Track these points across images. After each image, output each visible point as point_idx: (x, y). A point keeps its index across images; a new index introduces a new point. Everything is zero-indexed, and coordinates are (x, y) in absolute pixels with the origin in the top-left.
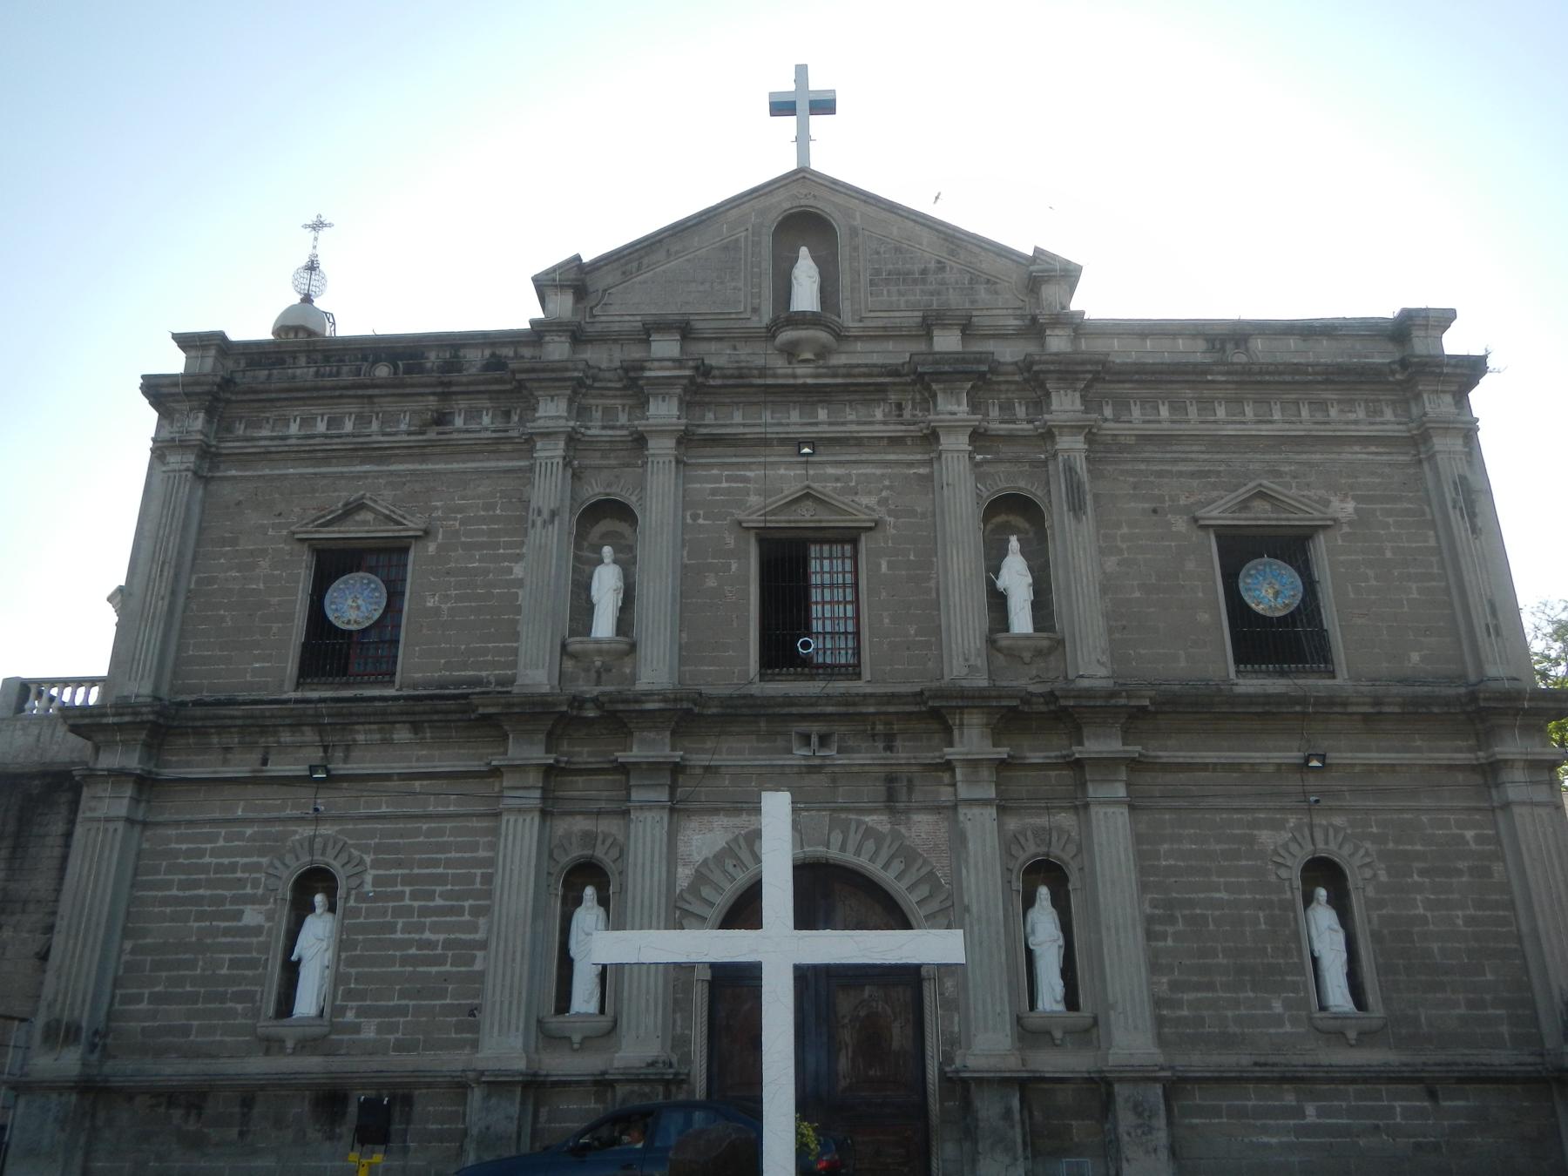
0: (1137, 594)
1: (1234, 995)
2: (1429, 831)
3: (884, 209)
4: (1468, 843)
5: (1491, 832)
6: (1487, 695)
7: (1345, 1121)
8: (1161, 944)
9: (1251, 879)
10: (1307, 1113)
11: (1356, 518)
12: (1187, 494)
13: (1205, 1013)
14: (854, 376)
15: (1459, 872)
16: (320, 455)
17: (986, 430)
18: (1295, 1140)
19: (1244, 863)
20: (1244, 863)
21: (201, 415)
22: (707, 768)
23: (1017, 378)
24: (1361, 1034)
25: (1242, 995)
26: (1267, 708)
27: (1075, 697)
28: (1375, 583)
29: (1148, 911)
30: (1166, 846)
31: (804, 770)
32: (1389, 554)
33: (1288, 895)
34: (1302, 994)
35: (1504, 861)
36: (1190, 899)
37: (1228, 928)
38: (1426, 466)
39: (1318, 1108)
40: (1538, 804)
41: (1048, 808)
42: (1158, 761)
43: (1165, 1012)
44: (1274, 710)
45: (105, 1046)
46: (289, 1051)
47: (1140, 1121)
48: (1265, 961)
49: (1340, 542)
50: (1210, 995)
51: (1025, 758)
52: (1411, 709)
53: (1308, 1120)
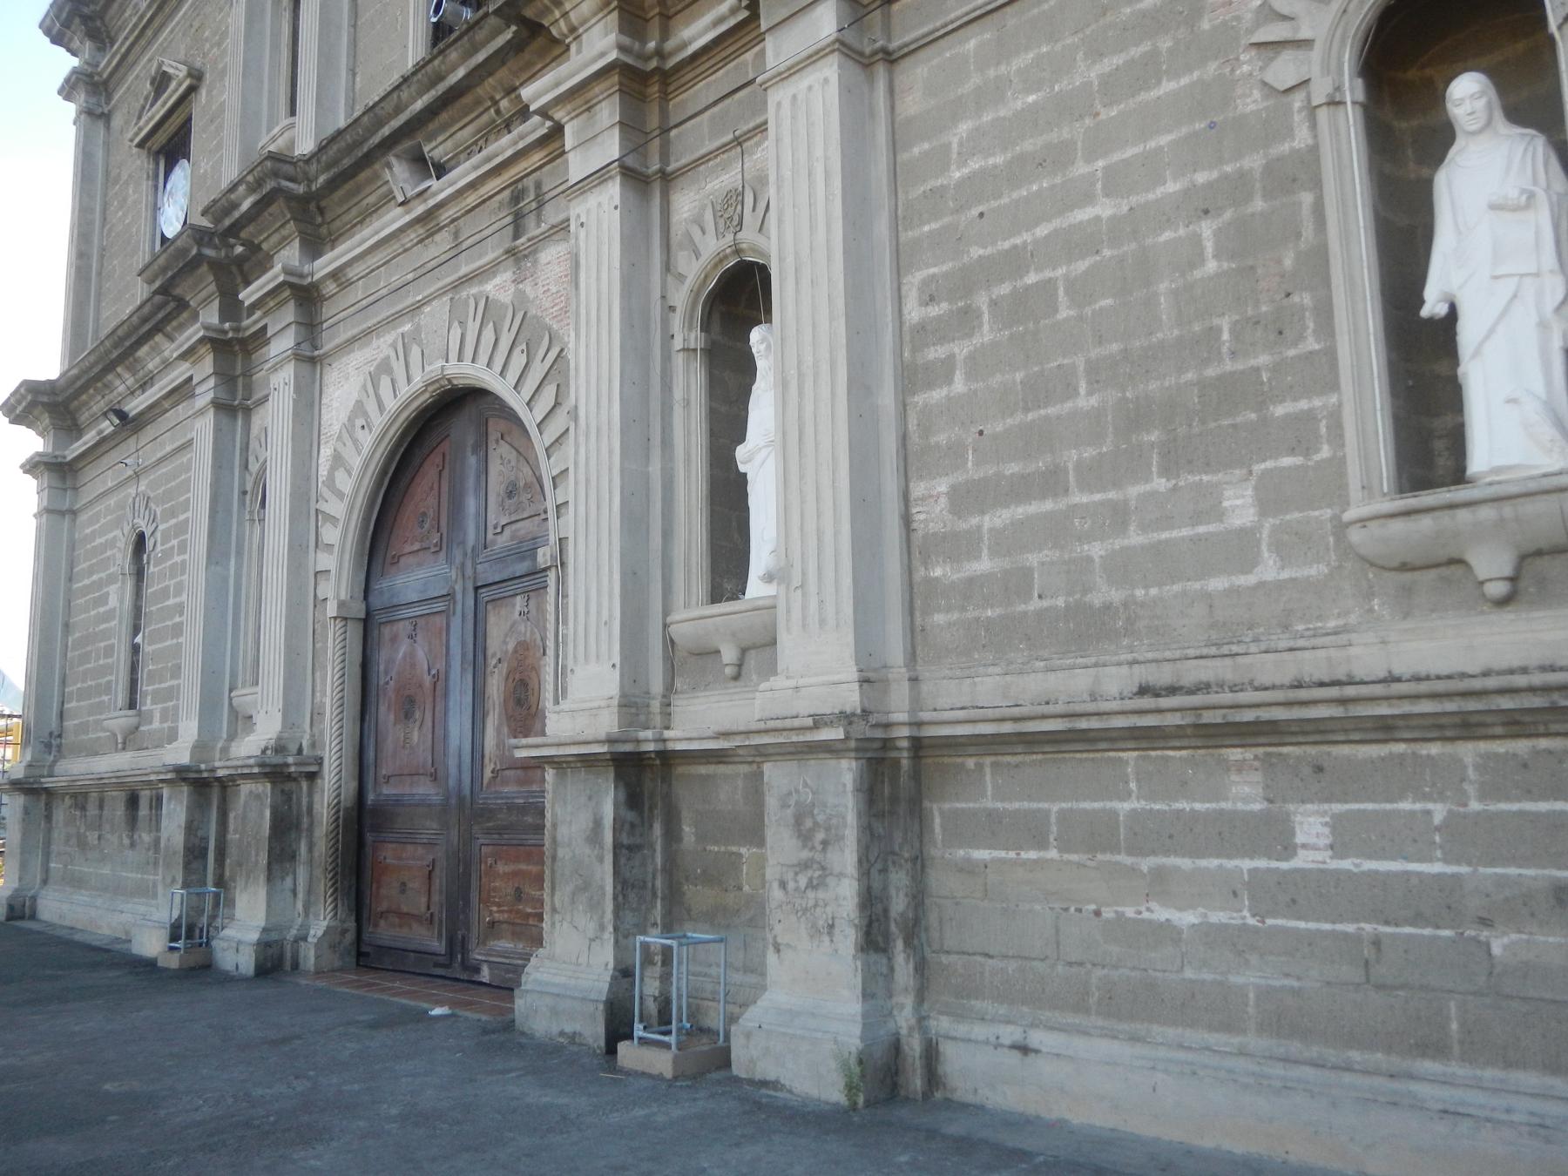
1: (1112, 495)
7: (1437, 868)
8: (937, 395)
9: (1184, 130)
10: (1300, 838)
13: (1033, 559)
16: (149, 33)
18: (1251, 921)
19: (1168, 86)
20: (1168, 86)
21: (88, 44)
22: (335, 275)
24: (1527, 557)
25: (1134, 491)
29: (914, 313)
30: (964, 128)
31: (420, 231)
33: (1302, 138)
34: (1325, 452)
36: (1015, 247)
37: (1108, 302)
39: (1338, 824)
41: (738, 142)
43: (938, 572)
45: (59, 746)
46: (120, 746)
47: (805, 854)
48: (1211, 372)
50: (1048, 505)
51: (684, 45)
53: (1304, 860)
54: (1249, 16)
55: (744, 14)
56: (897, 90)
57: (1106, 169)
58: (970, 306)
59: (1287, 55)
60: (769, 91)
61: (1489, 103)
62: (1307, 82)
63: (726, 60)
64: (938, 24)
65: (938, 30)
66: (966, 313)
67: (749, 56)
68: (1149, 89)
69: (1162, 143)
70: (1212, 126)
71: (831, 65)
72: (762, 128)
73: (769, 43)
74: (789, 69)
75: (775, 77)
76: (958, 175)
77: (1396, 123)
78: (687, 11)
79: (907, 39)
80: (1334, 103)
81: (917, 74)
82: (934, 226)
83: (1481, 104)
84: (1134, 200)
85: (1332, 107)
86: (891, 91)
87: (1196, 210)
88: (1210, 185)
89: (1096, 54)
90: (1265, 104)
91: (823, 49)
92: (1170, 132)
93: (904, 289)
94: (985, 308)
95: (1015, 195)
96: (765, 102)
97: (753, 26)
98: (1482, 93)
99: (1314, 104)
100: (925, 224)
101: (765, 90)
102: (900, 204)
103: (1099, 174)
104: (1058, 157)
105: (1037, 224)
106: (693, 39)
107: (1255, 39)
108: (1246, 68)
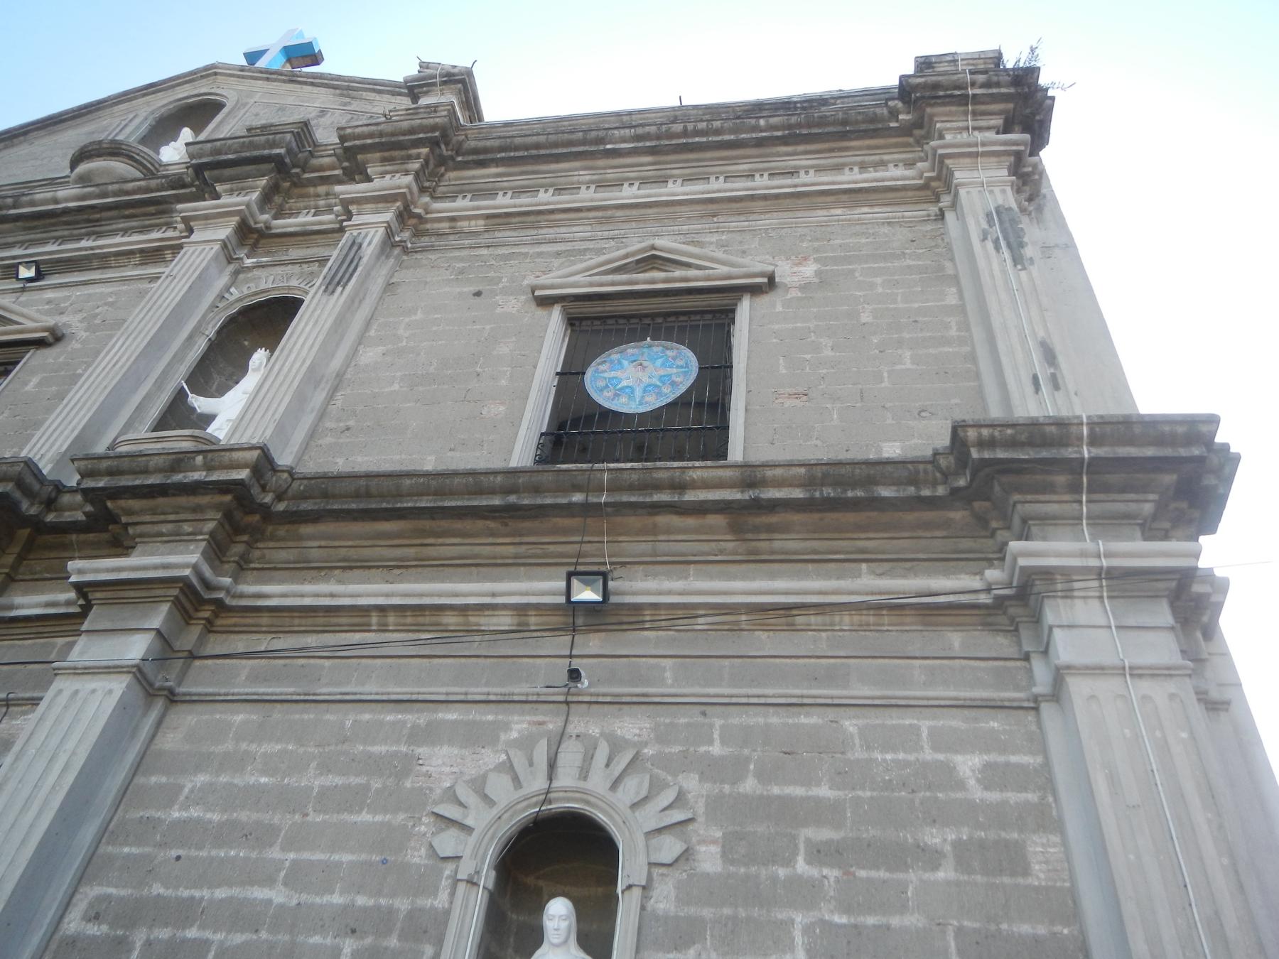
0: (396, 387)
2: (858, 754)
3: (284, 81)
4: (961, 785)
5: (1026, 759)
6: (985, 432)
9: (364, 857)
11: (816, 280)
12: (537, 274)
14: (127, 193)
15: (932, 858)
17: (268, 228)
19: (365, 817)
20: (365, 817)
23: (336, 172)
26: (512, 499)
27: (111, 473)
28: (831, 353)
29: (74, 924)
30: (202, 779)
32: (865, 318)
33: (441, 900)
35: (1058, 826)
36: (192, 898)
38: (950, 216)
40: (1137, 673)
42: (260, 603)
44: (526, 502)
49: (779, 308)
51: (11, 607)
52: (829, 492)
54: (438, 791)
55: (78, 610)
56: (164, 725)
57: (294, 862)
58: (127, 937)
59: (453, 832)
60: (58, 677)
61: (569, 927)
62: (459, 858)
63: (39, 635)
64: (223, 691)
65: (220, 695)
66: (119, 943)
67: (60, 641)
68: (351, 812)
69: (344, 860)
70: (384, 862)
71: (121, 683)
72: (35, 702)
73: (82, 641)
74: (86, 668)
75: (70, 669)
76: (176, 815)
77: (509, 913)
78: (31, 583)
79: (193, 690)
80: (472, 882)
81: (187, 720)
82: (135, 850)
83: (564, 925)
84: (304, 897)
85: (469, 885)
86: (159, 723)
87: (347, 926)
88: (365, 909)
89: (325, 768)
90: (426, 862)
91: (122, 667)
92: (352, 853)
93: (78, 896)
94: (138, 945)
95: (214, 853)
96: (51, 682)
97: (78, 621)
98: (567, 918)
99: (459, 877)
100: (127, 845)
101: (56, 675)
102: (115, 819)
103: (287, 864)
104: (261, 836)
105: (219, 886)
106: (17, 608)
107: (435, 810)
108: (423, 828)
